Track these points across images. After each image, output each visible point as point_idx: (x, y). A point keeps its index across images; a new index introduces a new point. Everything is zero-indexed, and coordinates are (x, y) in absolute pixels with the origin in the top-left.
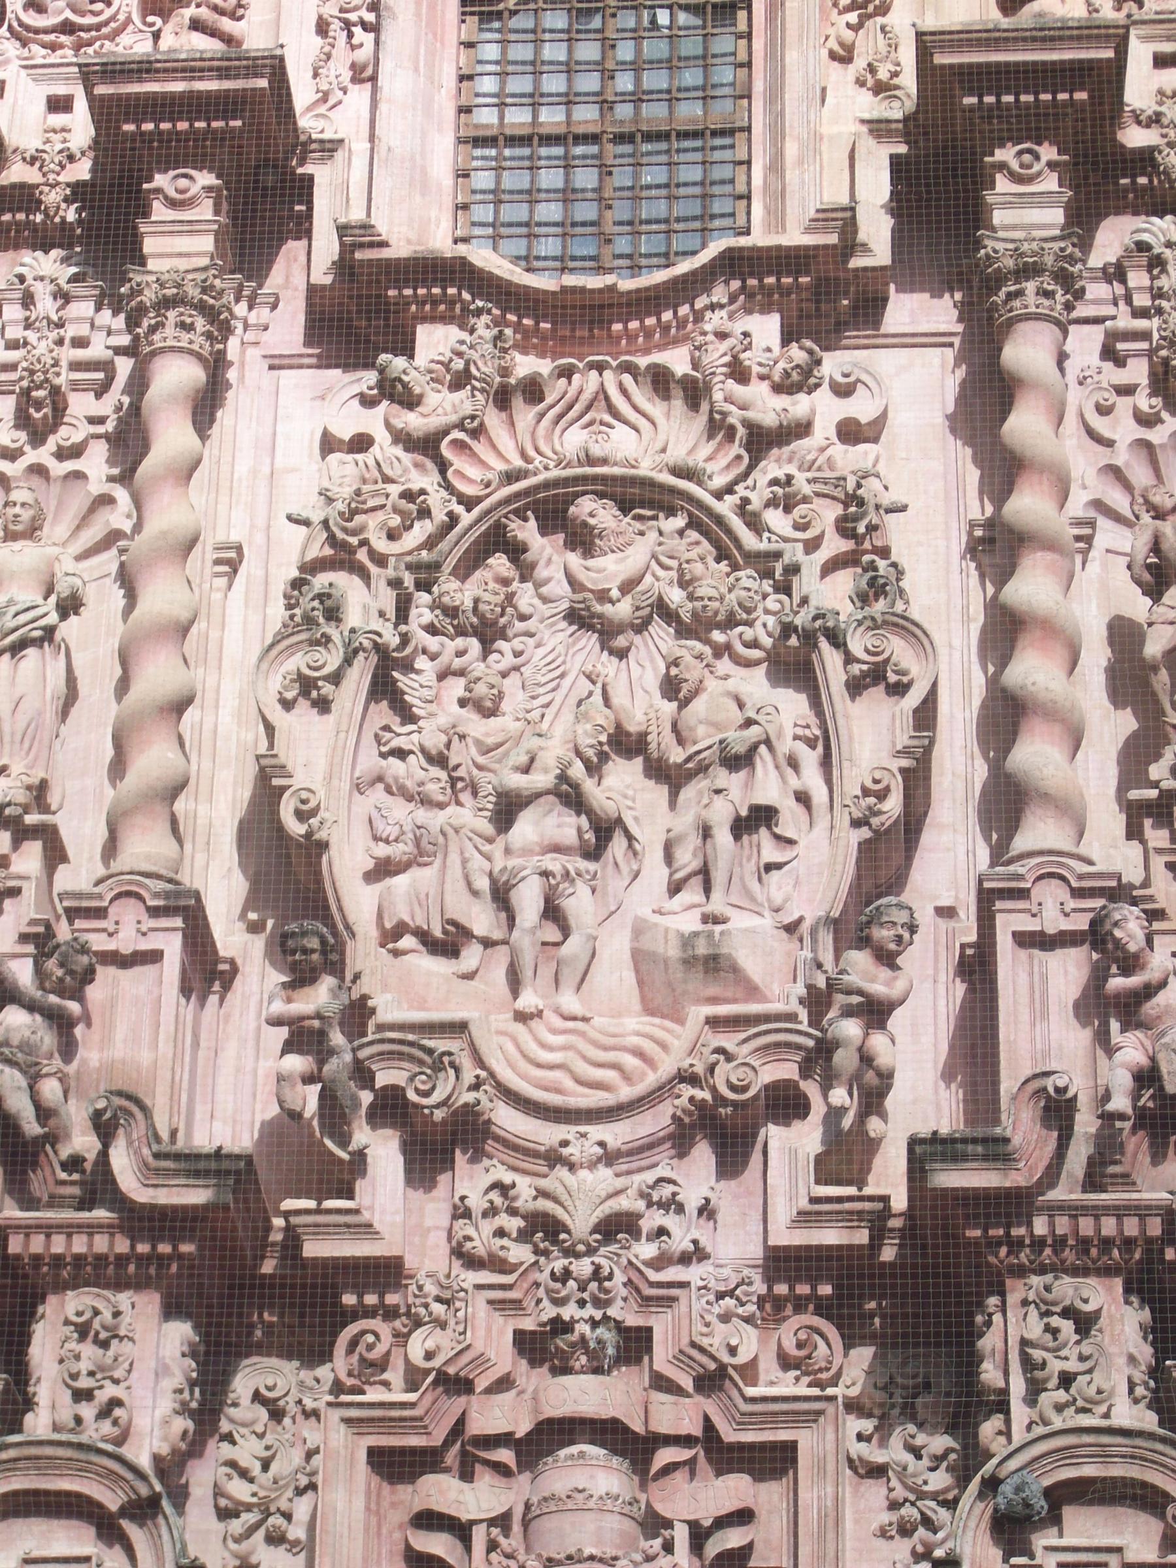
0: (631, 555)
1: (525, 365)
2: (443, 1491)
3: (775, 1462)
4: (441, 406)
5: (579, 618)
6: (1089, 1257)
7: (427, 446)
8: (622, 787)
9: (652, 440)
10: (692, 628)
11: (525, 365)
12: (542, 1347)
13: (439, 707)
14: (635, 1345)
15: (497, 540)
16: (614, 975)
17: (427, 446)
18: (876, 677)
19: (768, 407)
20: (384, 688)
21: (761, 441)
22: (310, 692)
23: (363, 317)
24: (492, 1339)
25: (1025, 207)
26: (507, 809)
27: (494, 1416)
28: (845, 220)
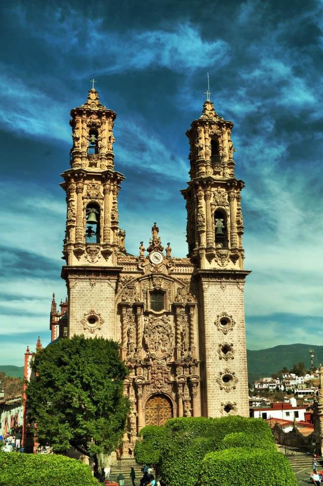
0: (160, 329)
1: (155, 318)
2: (154, 375)
3: (167, 374)
4: (151, 321)
5: (158, 332)
6: (181, 366)
7: (151, 323)
8: (160, 341)
9: (161, 323)
10: (163, 333)
11: (155, 318)
12: (158, 369)
13: (152, 336)
14: (162, 368)
15: (154, 328)
16: (160, 350)
17: (151, 323)
18: (172, 337)
19: (167, 321)
20: (150, 336)
21: (166, 323)
22: (146, 336)
23: (146, 314)
24: (156, 368)
25: (178, 311)
26: (156, 343)
27: (156, 372)
28: (169, 311)
